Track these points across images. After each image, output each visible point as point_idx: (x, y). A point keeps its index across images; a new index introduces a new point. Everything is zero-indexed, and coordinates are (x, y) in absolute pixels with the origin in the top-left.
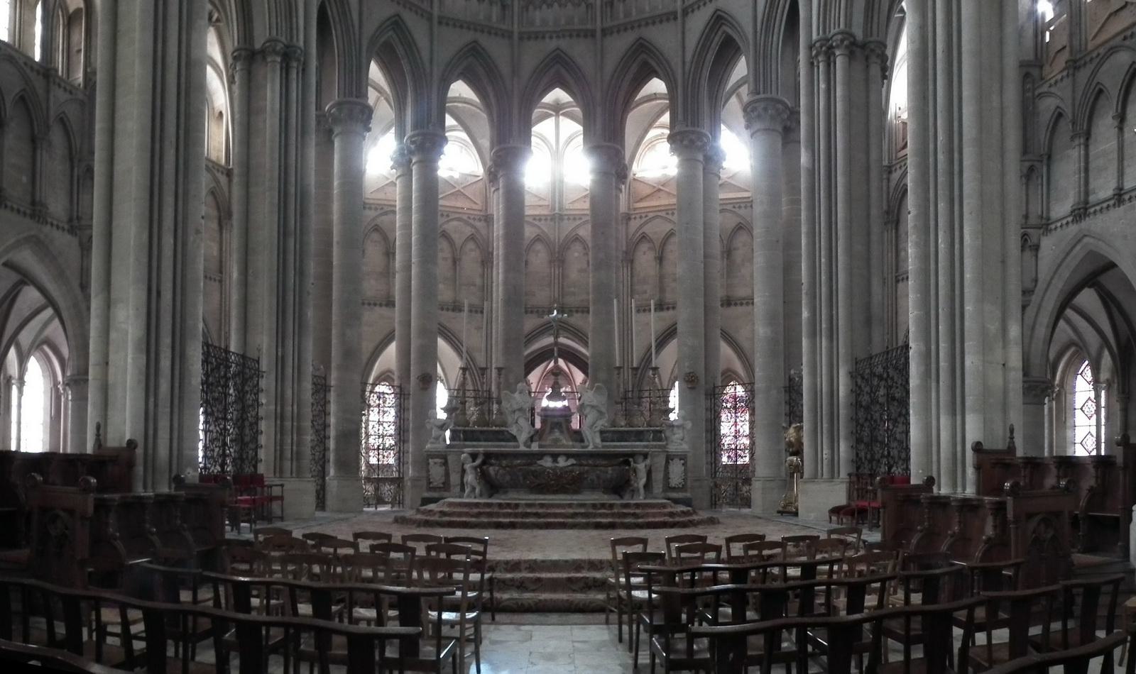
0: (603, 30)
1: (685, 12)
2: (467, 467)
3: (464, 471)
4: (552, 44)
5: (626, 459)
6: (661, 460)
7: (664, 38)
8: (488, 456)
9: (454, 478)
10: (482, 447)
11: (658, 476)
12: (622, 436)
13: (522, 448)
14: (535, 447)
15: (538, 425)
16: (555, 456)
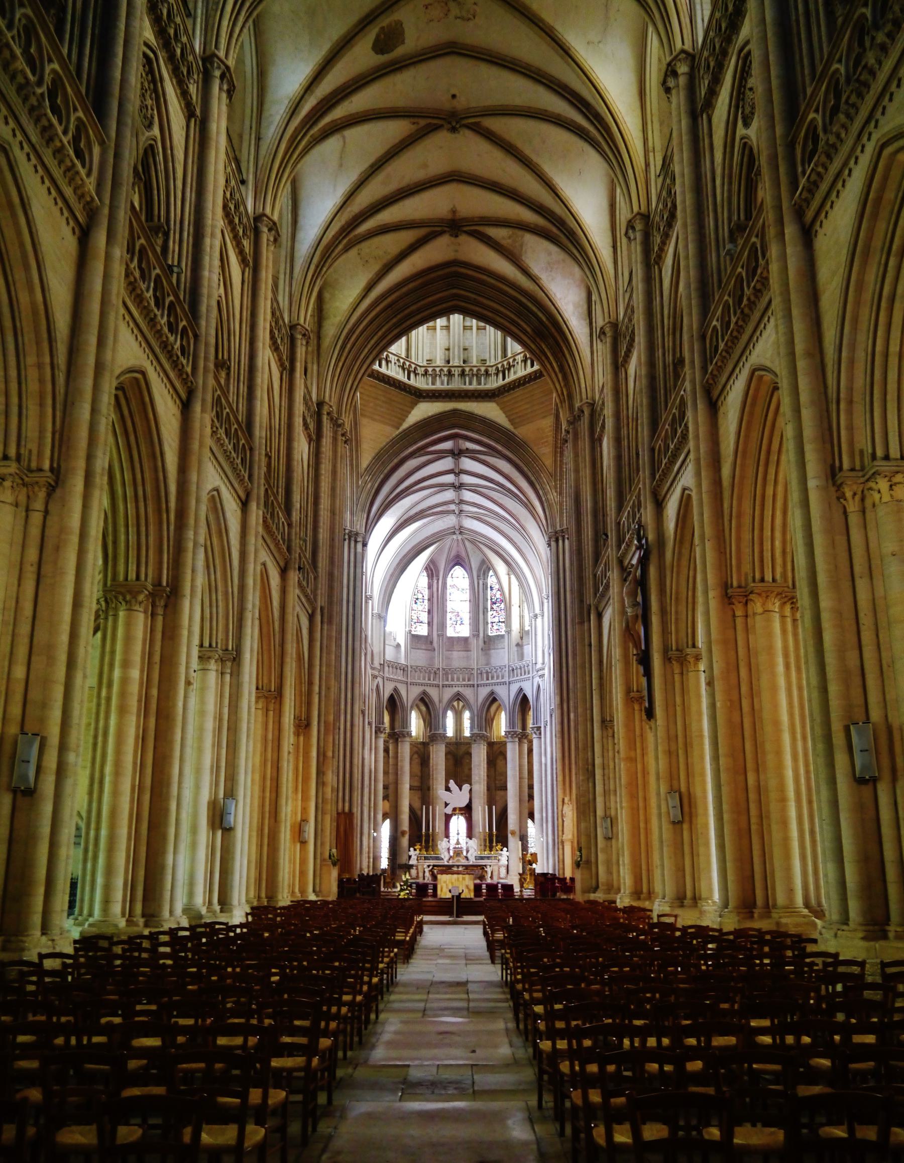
0: (478, 686)
1: (509, 683)
2: (427, 870)
3: (424, 872)
4: (455, 690)
5: (482, 867)
6: (496, 868)
7: (501, 692)
8: (434, 866)
9: (421, 875)
10: (432, 862)
11: (495, 874)
12: (482, 858)
13: (446, 863)
14: (451, 863)
15: (452, 854)
16: (458, 866)
